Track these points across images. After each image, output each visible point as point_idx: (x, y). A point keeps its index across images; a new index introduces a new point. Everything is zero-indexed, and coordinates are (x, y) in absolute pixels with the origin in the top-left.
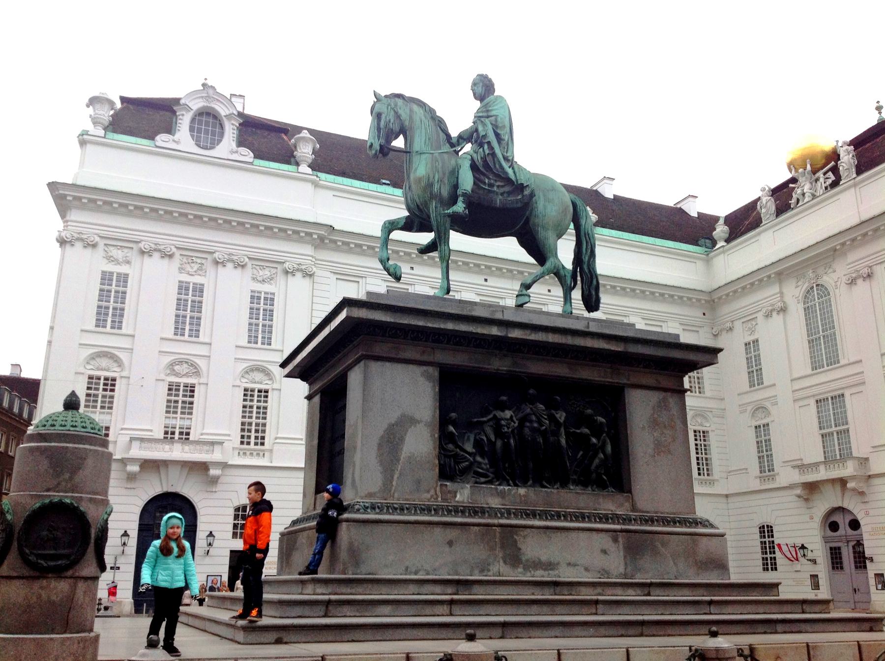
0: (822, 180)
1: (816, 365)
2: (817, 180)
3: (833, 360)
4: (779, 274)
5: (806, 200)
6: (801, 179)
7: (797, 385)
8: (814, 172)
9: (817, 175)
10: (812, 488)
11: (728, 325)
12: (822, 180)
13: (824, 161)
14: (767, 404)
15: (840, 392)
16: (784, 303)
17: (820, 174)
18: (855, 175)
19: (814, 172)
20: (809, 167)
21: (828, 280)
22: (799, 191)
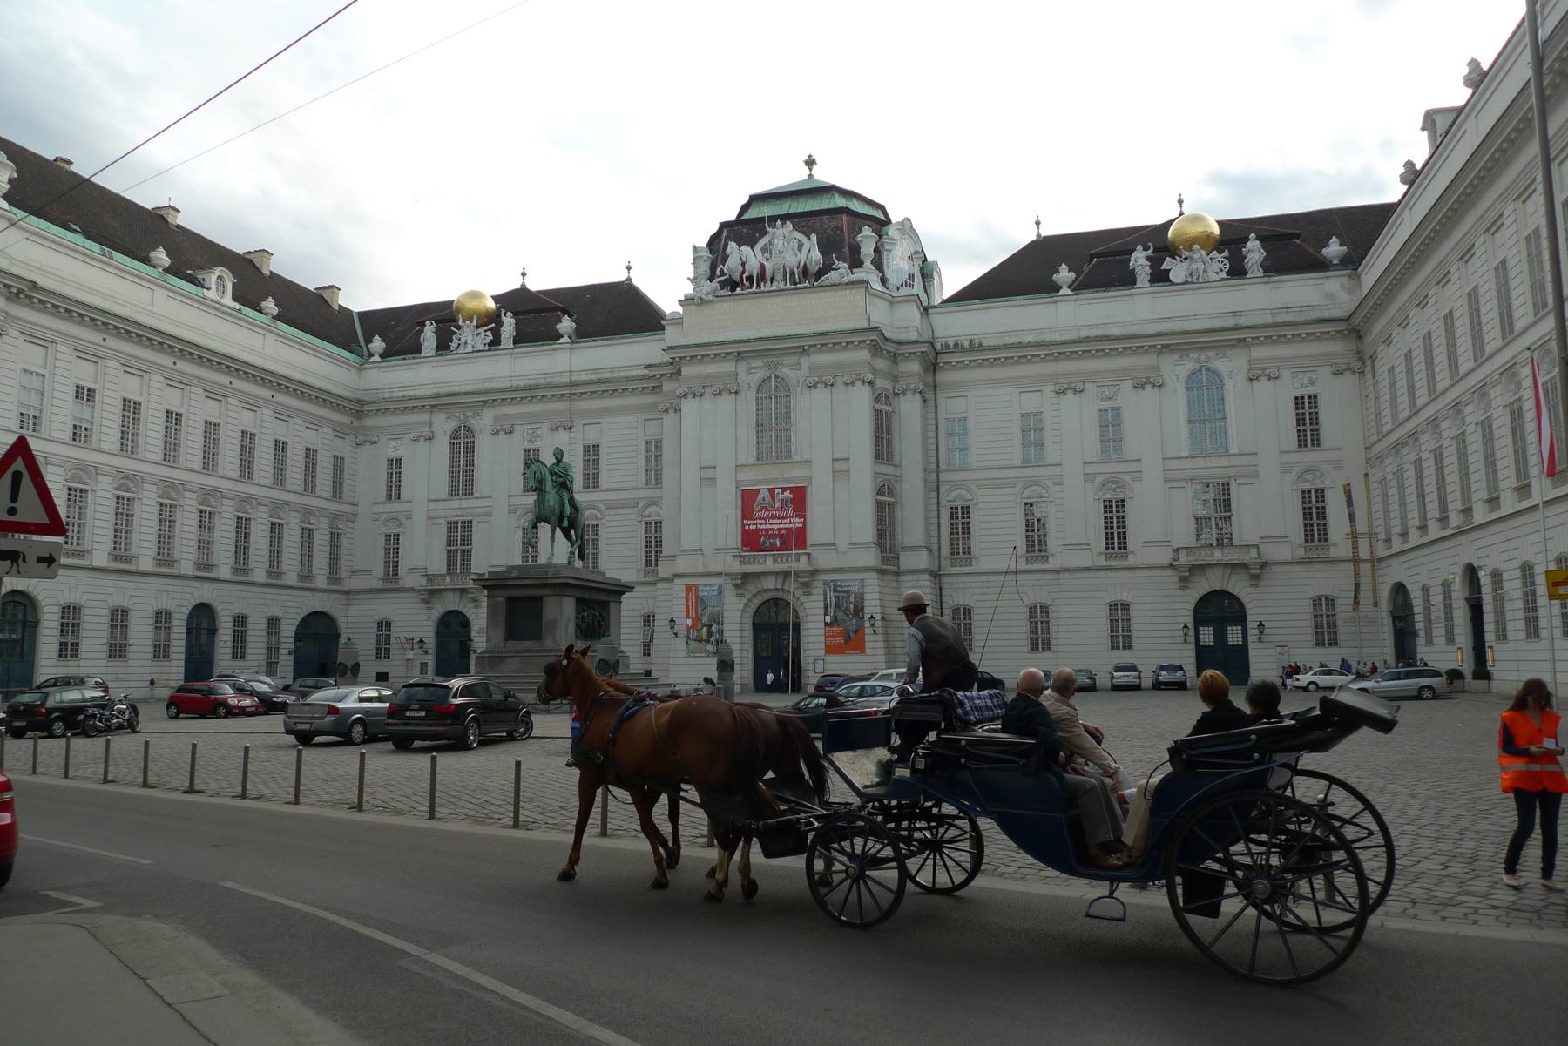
0: (483, 336)
1: (453, 493)
2: (478, 334)
3: (469, 491)
4: (432, 406)
5: (468, 350)
6: (465, 329)
7: (433, 505)
8: (477, 327)
9: (479, 330)
10: (433, 593)
11: (375, 439)
12: (483, 336)
13: (485, 320)
14: (402, 517)
15: (469, 518)
16: (432, 432)
17: (482, 330)
18: (512, 346)
19: (477, 327)
20: (475, 323)
21: (475, 423)
22: (463, 340)
